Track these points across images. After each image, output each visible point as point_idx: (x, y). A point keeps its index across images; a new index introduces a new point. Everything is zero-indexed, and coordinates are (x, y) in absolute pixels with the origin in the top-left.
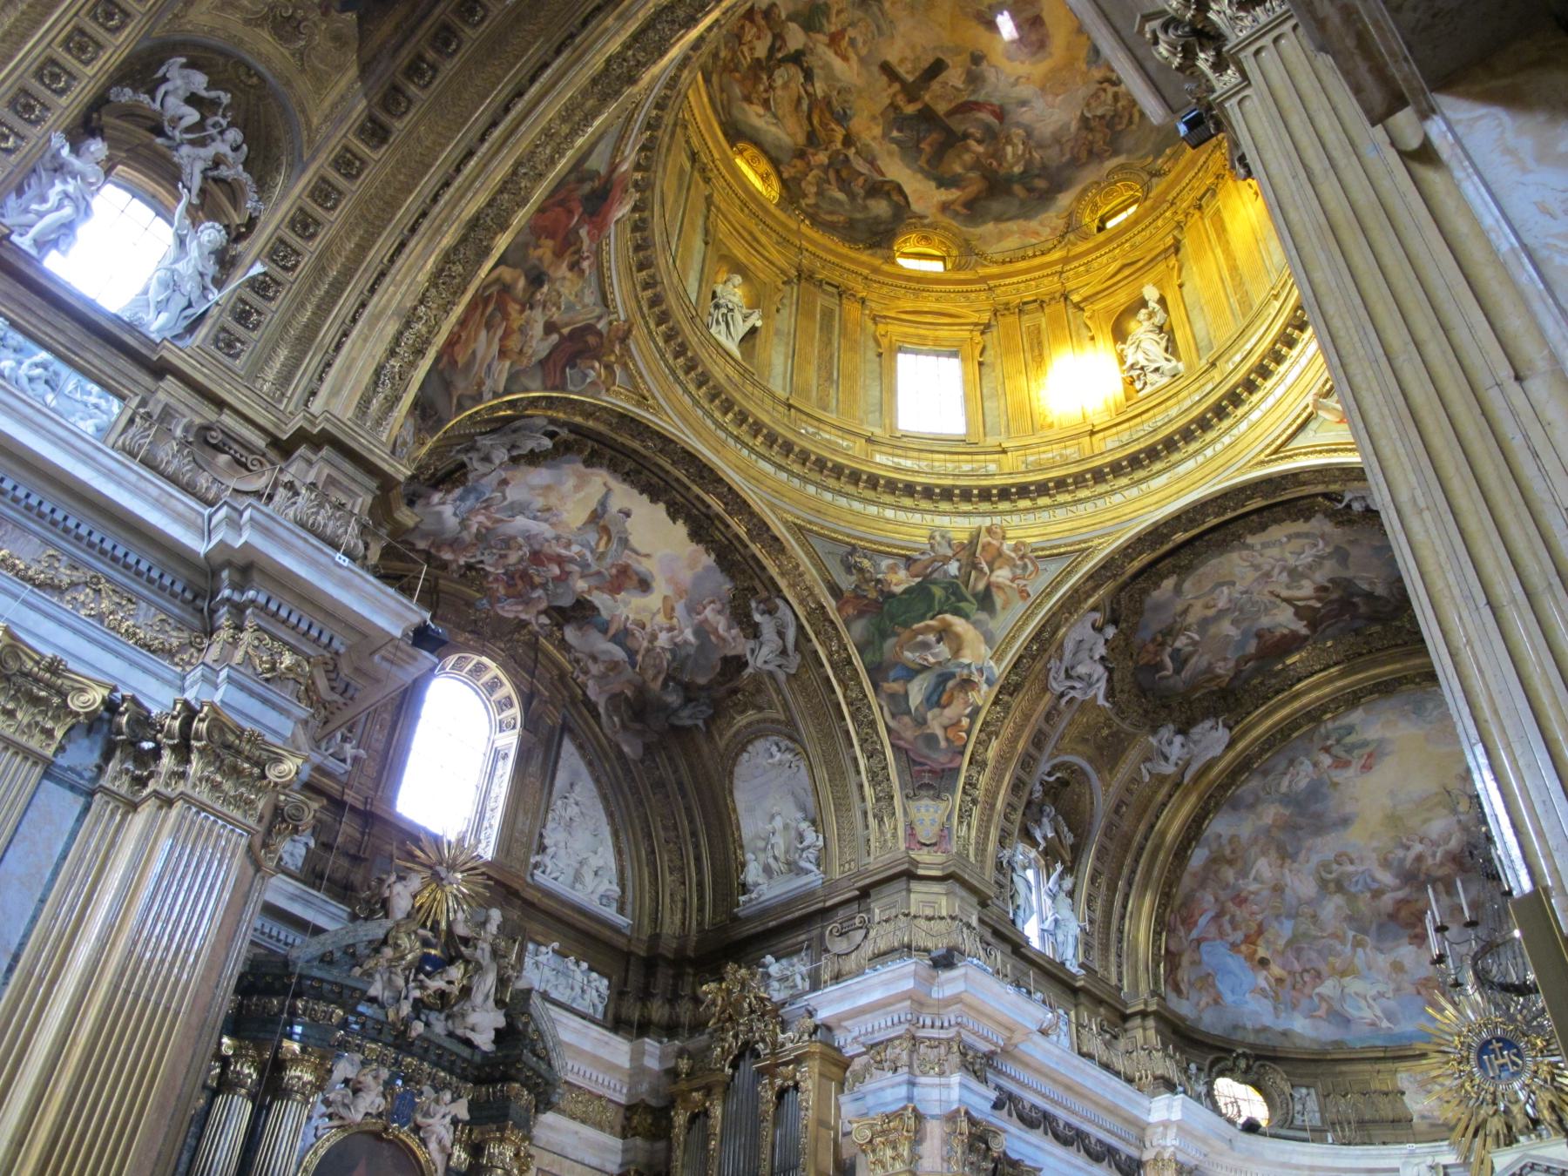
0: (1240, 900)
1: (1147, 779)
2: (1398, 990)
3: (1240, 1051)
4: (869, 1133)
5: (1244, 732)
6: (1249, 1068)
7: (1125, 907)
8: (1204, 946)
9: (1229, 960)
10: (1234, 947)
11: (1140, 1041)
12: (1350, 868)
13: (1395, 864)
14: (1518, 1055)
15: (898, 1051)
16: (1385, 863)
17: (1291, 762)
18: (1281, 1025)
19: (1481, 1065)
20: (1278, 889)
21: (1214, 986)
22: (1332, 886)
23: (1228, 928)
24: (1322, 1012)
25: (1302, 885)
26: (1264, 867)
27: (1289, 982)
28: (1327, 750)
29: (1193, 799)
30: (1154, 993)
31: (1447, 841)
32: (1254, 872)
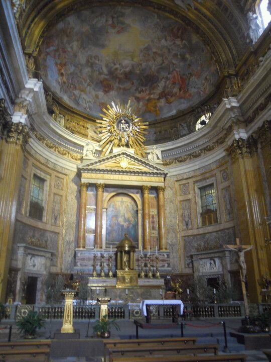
2: (95, 102)
7: (33, 19)
8: (49, 56)
9: (53, 67)
10: (56, 64)
12: (97, 62)
16: (107, 66)
17: (101, 14)
20: (75, 55)
21: (47, 71)
22: (90, 64)
26: (75, 45)
27: (67, 84)
28: (113, 18)
31: (126, 68)
32: (70, 45)
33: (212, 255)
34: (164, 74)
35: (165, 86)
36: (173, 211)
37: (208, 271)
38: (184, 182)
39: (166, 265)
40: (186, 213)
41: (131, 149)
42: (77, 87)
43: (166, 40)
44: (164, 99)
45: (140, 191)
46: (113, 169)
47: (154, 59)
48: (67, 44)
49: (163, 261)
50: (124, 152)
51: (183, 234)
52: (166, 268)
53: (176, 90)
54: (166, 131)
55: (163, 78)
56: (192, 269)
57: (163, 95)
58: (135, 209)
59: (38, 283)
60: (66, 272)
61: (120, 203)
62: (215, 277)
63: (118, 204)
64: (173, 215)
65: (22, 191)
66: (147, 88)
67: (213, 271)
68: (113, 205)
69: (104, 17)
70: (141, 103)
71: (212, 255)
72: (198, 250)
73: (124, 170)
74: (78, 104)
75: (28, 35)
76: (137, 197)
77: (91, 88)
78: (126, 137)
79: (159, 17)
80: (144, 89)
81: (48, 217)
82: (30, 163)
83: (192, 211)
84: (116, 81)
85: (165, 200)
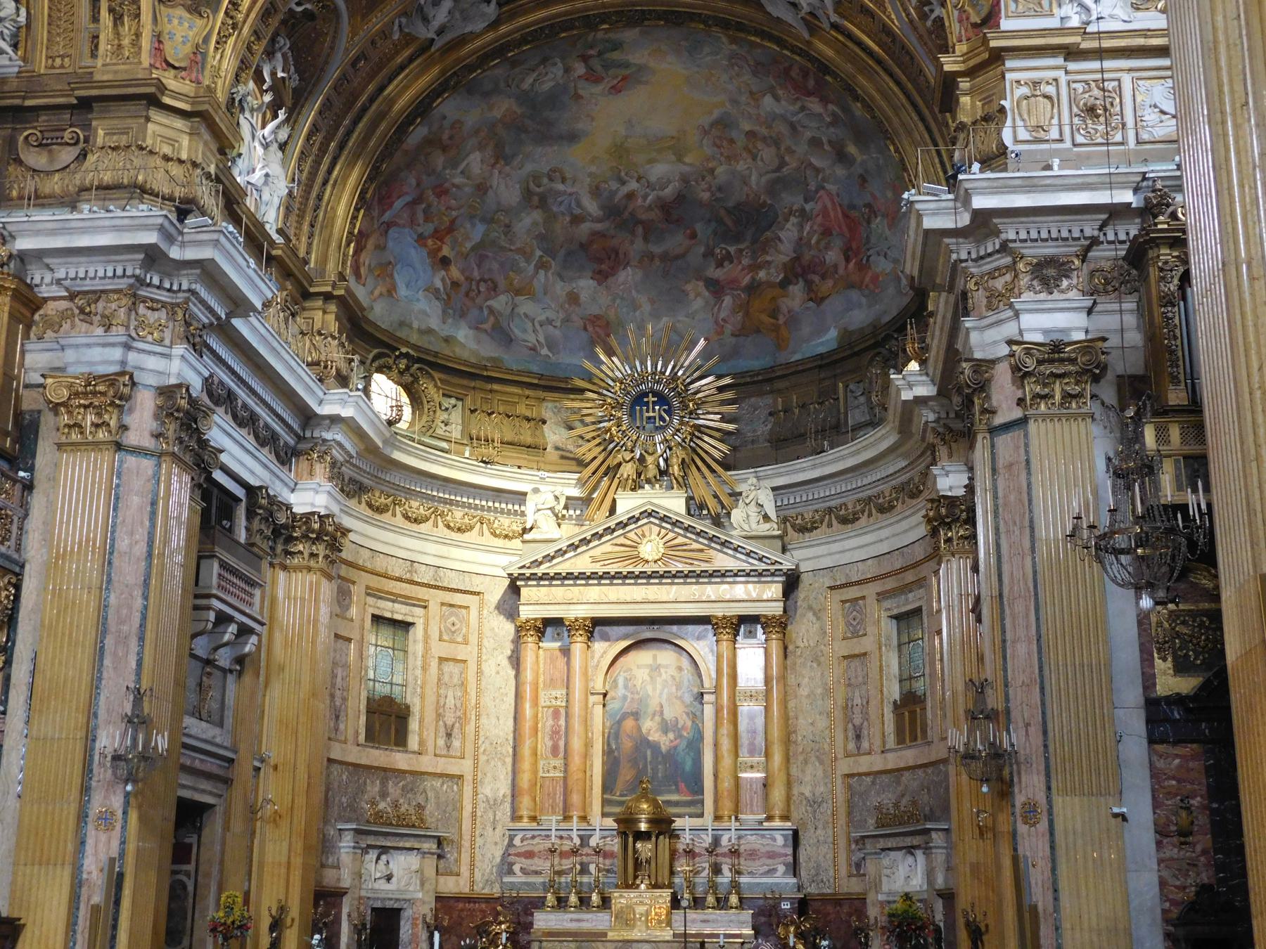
0: (441, 192)
1: (396, 36)
2: (567, 320)
3: (404, 350)
4: (66, 393)
5: (513, 15)
6: (408, 368)
7: (330, 172)
8: (393, 232)
9: (413, 251)
10: (421, 239)
11: (317, 326)
12: (561, 187)
13: (606, 194)
14: (669, 412)
15: (114, 306)
16: (596, 192)
17: (544, 61)
18: (446, 330)
19: (632, 414)
20: (482, 189)
21: (391, 276)
22: (536, 199)
23: (420, 217)
24: (487, 326)
25: (507, 191)
26: (475, 162)
27: (463, 289)
28: (585, 59)
29: (435, 71)
30: (342, 277)
33: (908, 841)
34: (792, 200)
35: (801, 239)
36: (819, 691)
38: (852, 593)
39: (781, 869)
40: (858, 701)
41: (675, 492)
42: (502, 284)
43: (777, 98)
44: (801, 283)
46: (612, 569)
47: (750, 151)
48: (447, 171)
49: (772, 855)
50: (649, 508)
51: (844, 766)
52: (781, 879)
53: (833, 256)
54: (803, 406)
55: (791, 213)
57: (798, 270)
58: (696, 690)
59: (402, 923)
60: (486, 891)
61: (647, 671)
63: (642, 675)
65: (339, 679)
66: (742, 246)
69: (555, 64)
70: (728, 301)
72: (880, 825)
73: (648, 569)
74: (503, 336)
75: (318, 226)
76: (703, 646)
77: (550, 274)
78: (660, 449)
79: (733, 40)
80: (732, 249)
82: (357, 591)
84: (633, 233)
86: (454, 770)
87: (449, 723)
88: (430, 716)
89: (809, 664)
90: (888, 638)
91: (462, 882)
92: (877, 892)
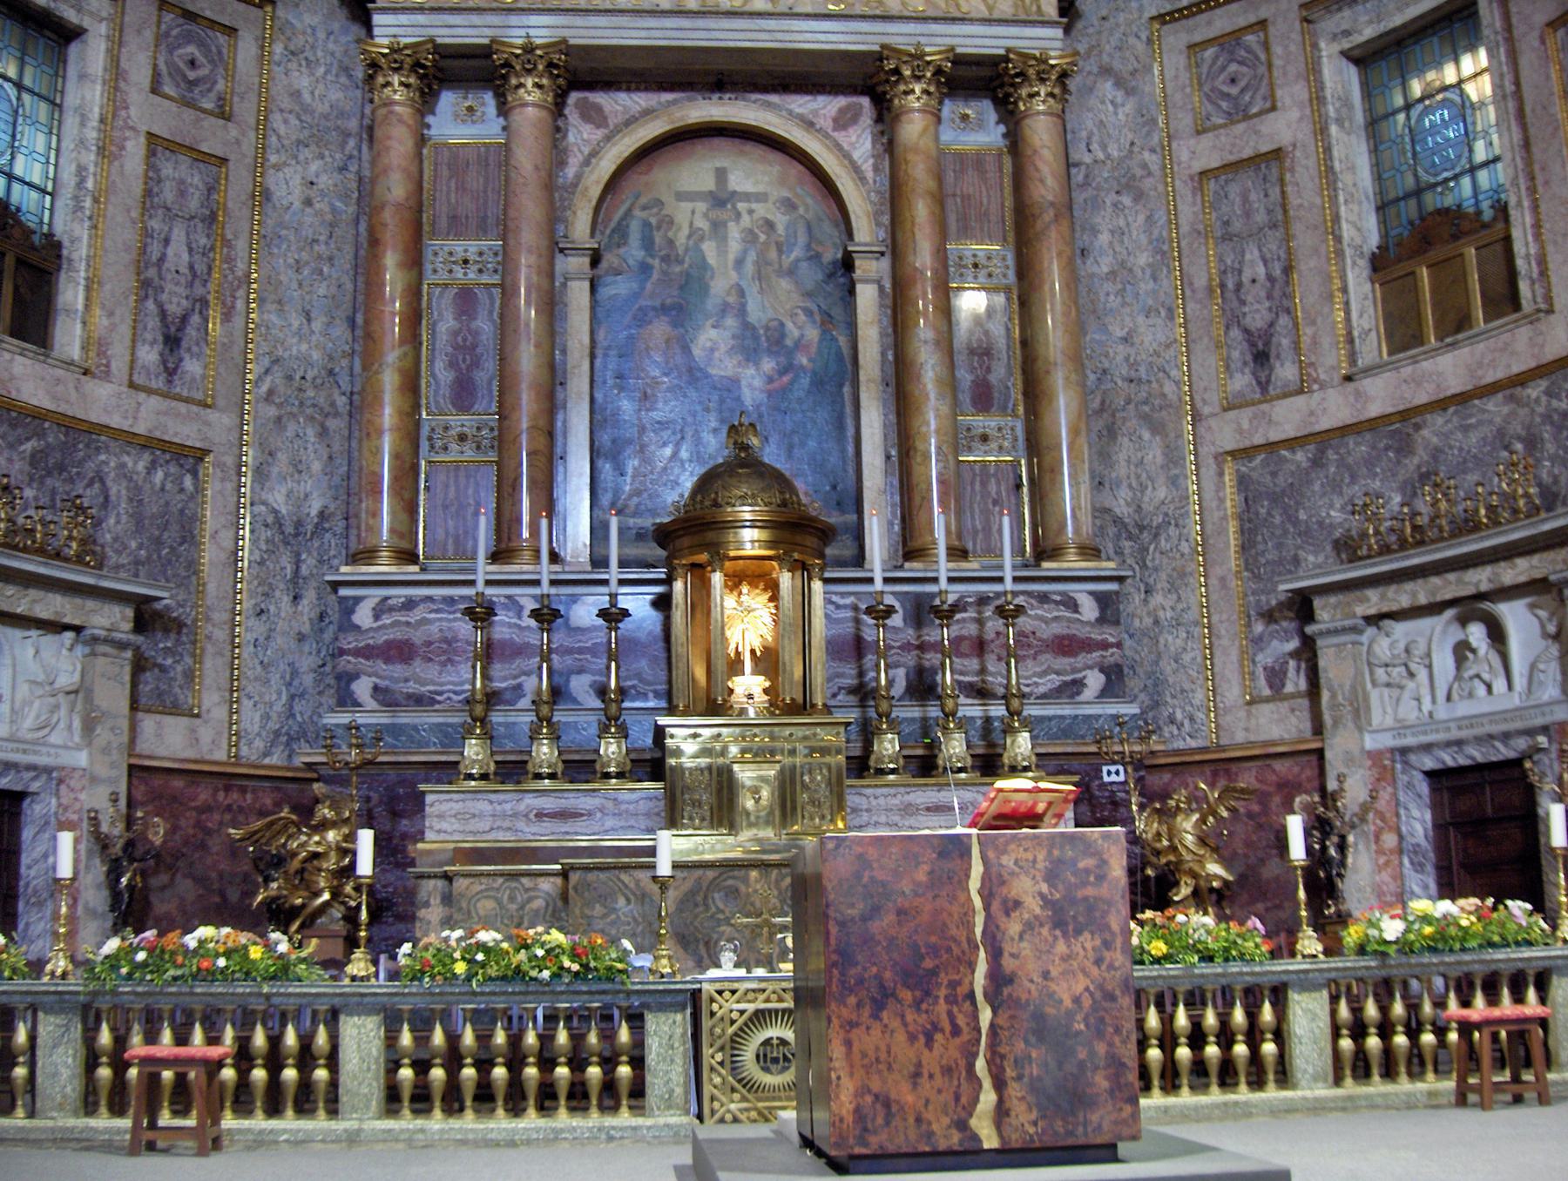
33: (1480, 578)
36: (1143, 259)
37: (1442, 713)
39: (1095, 681)
45: (865, 102)
49: (1067, 646)
51: (1226, 433)
52: (1091, 704)
56: (1305, 702)
58: (832, 254)
59: (27, 834)
60: (274, 760)
61: (701, 207)
62: (1504, 752)
63: (688, 217)
64: (1146, 286)
67: (1481, 704)
68: (646, 224)
71: (1480, 578)
81: (100, 319)
83: (1304, 239)
85: (1078, 176)
86: (184, 432)
87: (175, 307)
88: (119, 280)
89: (1112, 197)
90: (1346, 102)
91: (206, 734)
92: (1360, 729)
